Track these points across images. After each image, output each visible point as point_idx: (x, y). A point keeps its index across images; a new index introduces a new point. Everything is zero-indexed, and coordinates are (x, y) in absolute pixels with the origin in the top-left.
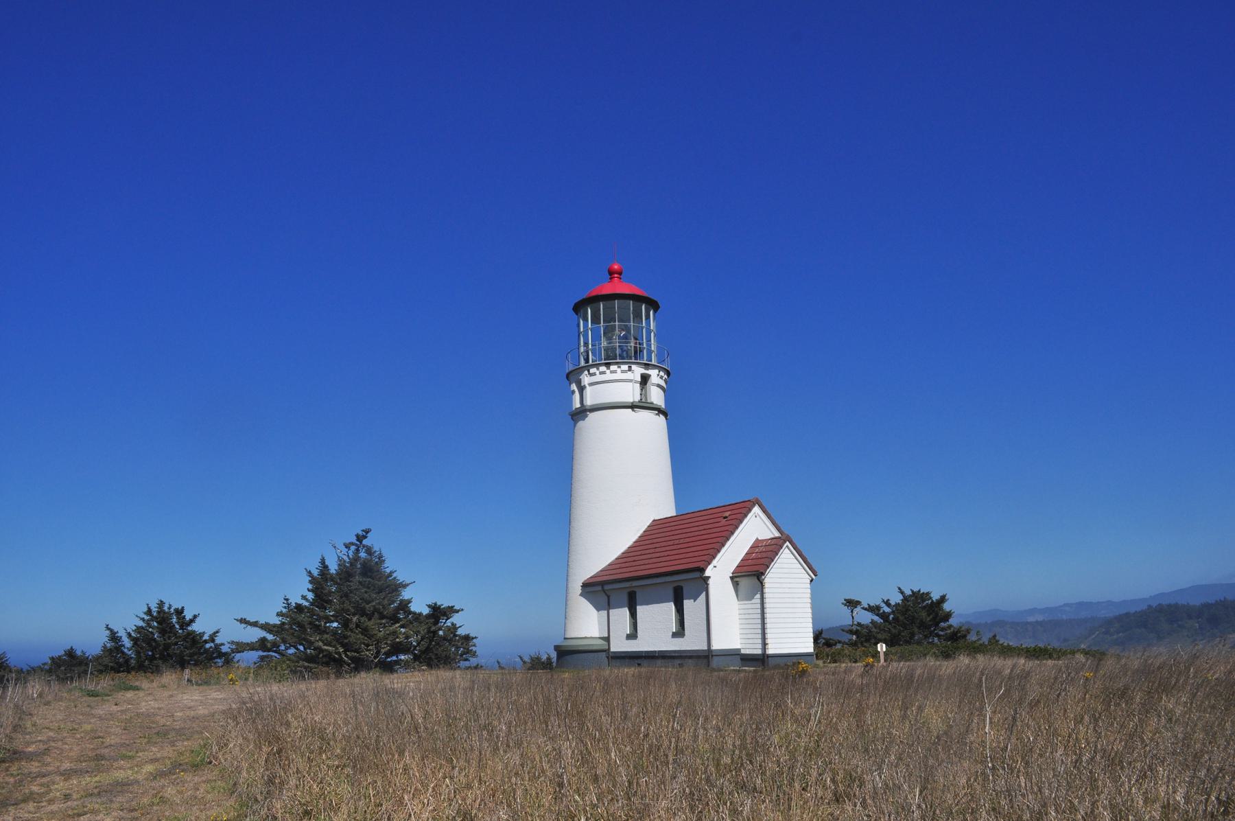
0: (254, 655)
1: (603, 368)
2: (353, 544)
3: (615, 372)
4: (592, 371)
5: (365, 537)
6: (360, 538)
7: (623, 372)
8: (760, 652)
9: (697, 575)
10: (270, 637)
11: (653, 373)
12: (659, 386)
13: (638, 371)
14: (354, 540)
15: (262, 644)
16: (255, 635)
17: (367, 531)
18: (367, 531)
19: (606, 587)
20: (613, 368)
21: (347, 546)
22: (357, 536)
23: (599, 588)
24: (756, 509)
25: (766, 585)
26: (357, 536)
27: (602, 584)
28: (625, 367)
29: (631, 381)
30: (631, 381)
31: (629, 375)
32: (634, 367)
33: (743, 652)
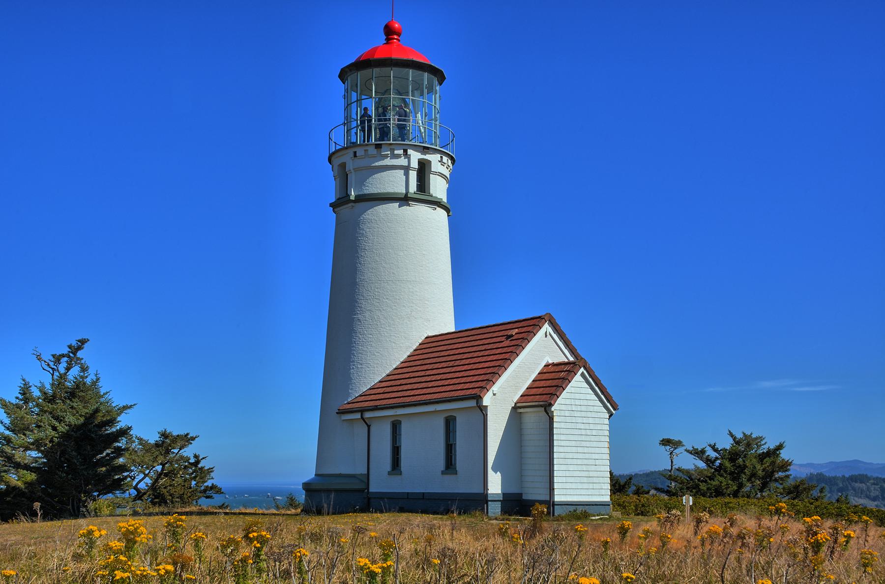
2: (63, 356)
5: (79, 348)
6: (75, 350)
9: (473, 403)
11: (434, 158)
12: (442, 175)
13: (415, 156)
14: (66, 350)
17: (83, 342)
19: (367, 415)
21: (57, 359)
22: (70, 347)
23: (358, 416)
24: (547, 327)
27: (362, 411)
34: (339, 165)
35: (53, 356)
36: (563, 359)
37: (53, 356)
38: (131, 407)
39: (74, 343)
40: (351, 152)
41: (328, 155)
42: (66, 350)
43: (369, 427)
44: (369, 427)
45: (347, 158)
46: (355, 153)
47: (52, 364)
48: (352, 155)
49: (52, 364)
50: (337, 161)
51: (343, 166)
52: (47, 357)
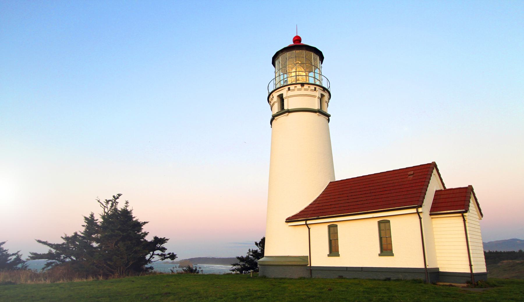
0: (44, 261)
1: (299, 86)
2: (110, 200)
3: (305, 90)
4: (292, 87)
5: (118, 198)
7: (312, 90)
8: (469, 271)
10: (54, 251)
14: (111, 198)
15: (50, 256)
16: (45, 250)
17: (119, 195)
18: (119, 195)
19: (308, 222)
20: (306, 86)
21: (107, 202)
22: (114, 197)
23: (304, 223)
25: (467, 221)
26: (114, 197)
28: (313, 87)
29: (314, 96)
30: (314, 96)
31: (314, 93)
32: (317, 88)
33: (441, 270)
34: (279, 96)
35: (106, 200)
36: (439, 189)
37: (106, 200)
38: (147, 223)
39: (116, 195)
40: (287, 88)
41: (267, 95)
42: (111, 198)
43: (309, 229)
44: (309, 229)
45: (284, 91)
46: (289, 89)
47: (104, 204)
48: (287, 89)
49: (104, 204)
50: (275, 95)
51: (281, 97)
52: (103, 201)
